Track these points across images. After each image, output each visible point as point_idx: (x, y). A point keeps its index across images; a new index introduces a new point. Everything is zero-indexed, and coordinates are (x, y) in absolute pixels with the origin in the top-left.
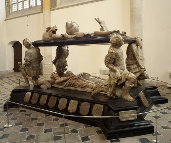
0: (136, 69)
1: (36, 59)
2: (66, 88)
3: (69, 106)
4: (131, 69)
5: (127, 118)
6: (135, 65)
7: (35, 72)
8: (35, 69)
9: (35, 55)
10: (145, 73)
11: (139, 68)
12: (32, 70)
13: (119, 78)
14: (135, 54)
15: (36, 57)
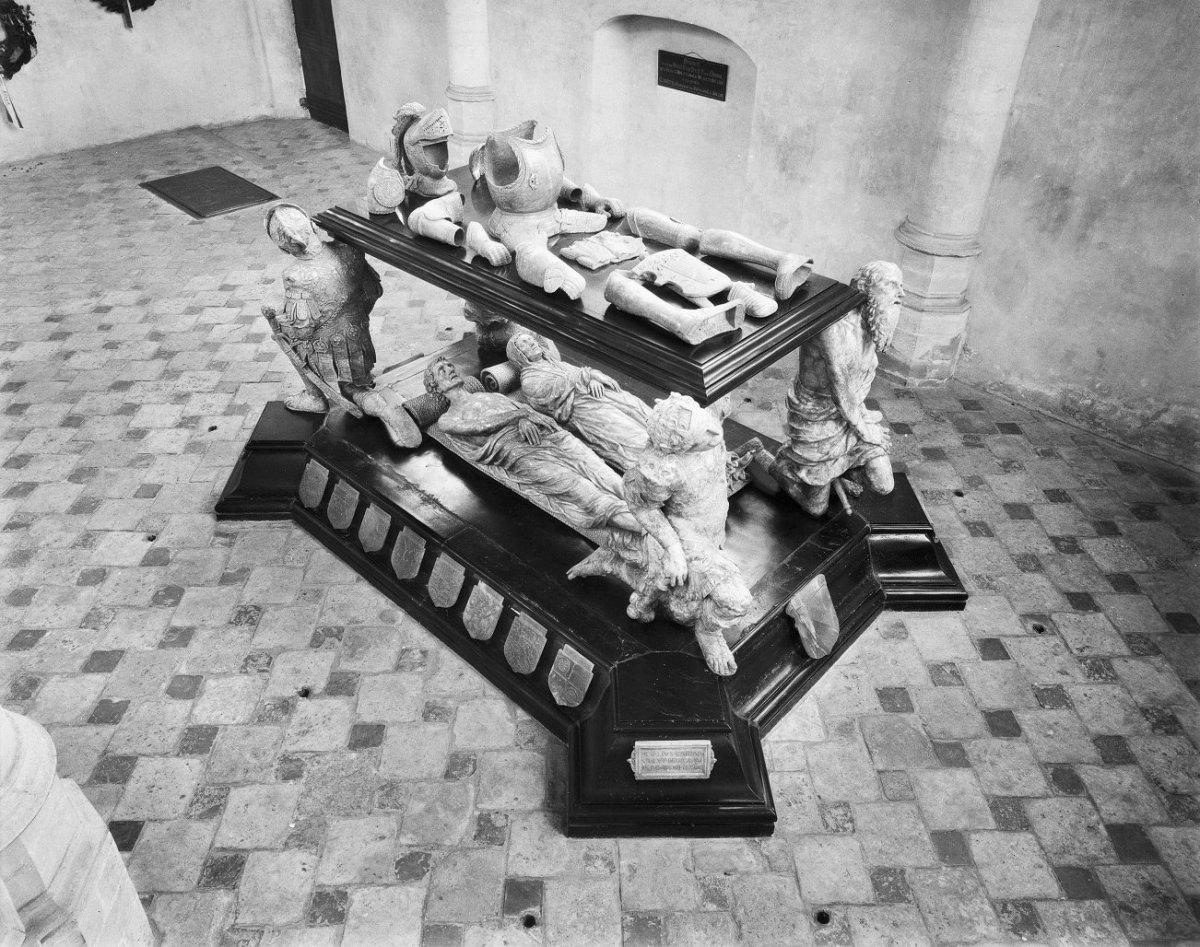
0: (833, 445)
1: (345, 306)
2: (483, 468)
3: (468, 604)
4: (804, 443)
5: (665, 768)
6: (831, 425)
7: (344, 363)
8: (344, 351)
9: (332, 290)
10: (873, 470)
11: (853, 440)
12: (330, 357)
13: (677, 581)
14: (837, 382)
15: (344, 297)
